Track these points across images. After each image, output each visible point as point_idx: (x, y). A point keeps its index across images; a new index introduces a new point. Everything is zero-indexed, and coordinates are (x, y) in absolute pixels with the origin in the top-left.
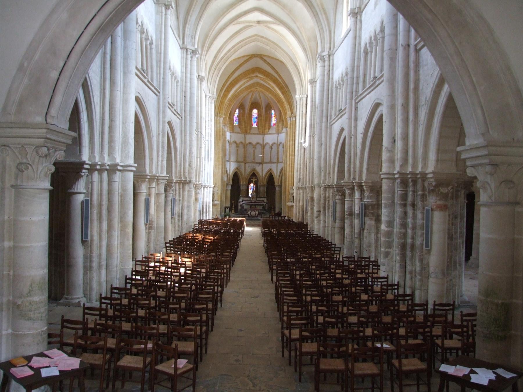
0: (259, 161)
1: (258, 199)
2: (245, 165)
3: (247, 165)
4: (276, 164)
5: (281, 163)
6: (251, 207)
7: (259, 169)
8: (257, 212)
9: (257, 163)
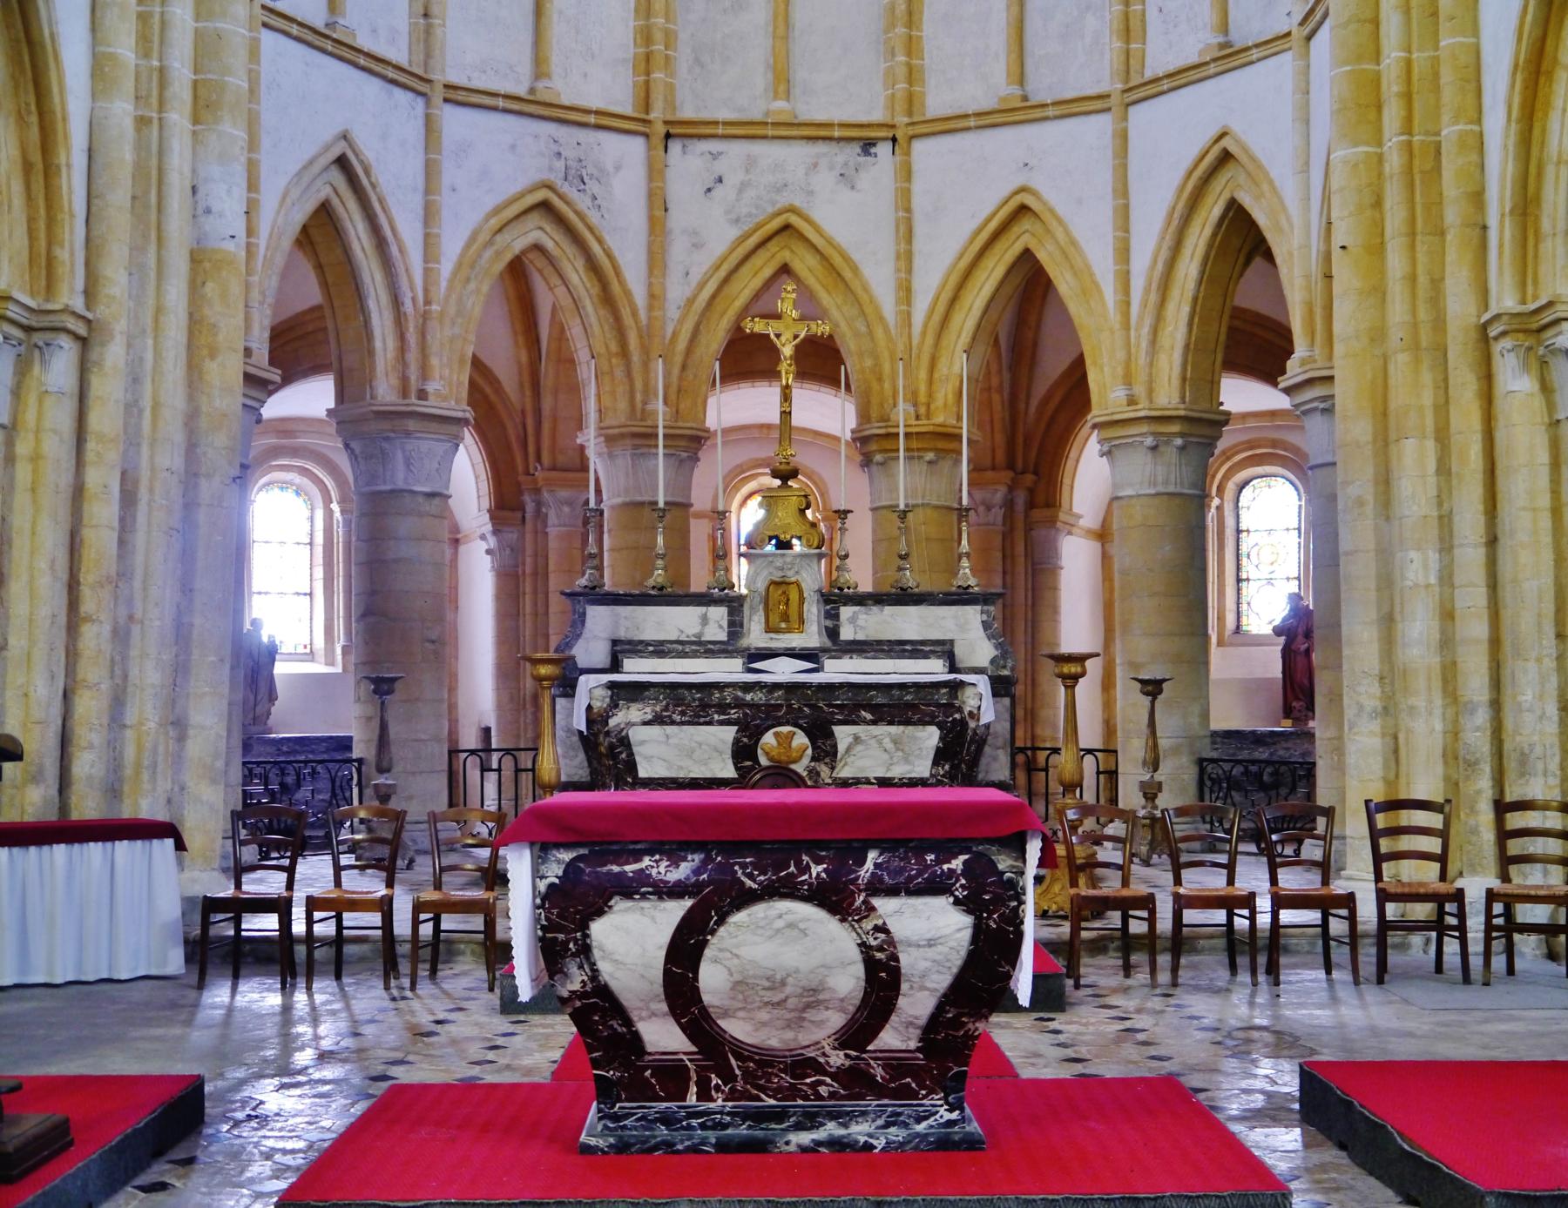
0: (867, 103)
1: (857, 623)
2: (655, 172)
3: (686, 163)
4: (1098, 127)
5: (1183, 77)
6: (743, 752)
7: (848, 209)
8: (931, 931)
9: (819, 133)
